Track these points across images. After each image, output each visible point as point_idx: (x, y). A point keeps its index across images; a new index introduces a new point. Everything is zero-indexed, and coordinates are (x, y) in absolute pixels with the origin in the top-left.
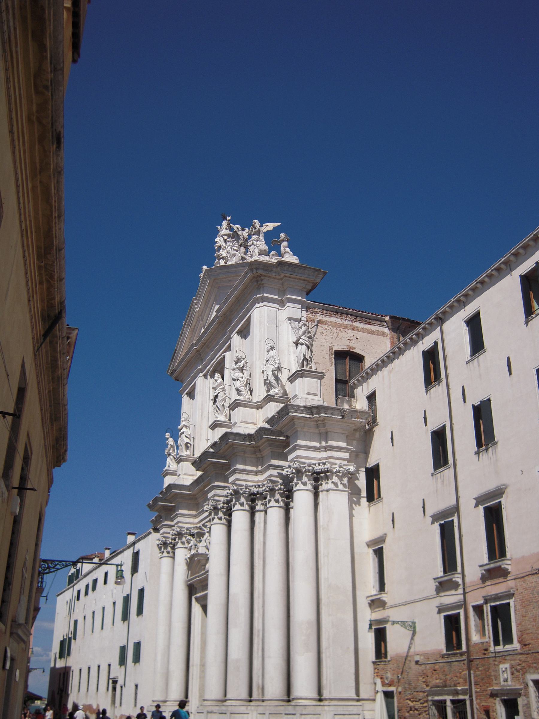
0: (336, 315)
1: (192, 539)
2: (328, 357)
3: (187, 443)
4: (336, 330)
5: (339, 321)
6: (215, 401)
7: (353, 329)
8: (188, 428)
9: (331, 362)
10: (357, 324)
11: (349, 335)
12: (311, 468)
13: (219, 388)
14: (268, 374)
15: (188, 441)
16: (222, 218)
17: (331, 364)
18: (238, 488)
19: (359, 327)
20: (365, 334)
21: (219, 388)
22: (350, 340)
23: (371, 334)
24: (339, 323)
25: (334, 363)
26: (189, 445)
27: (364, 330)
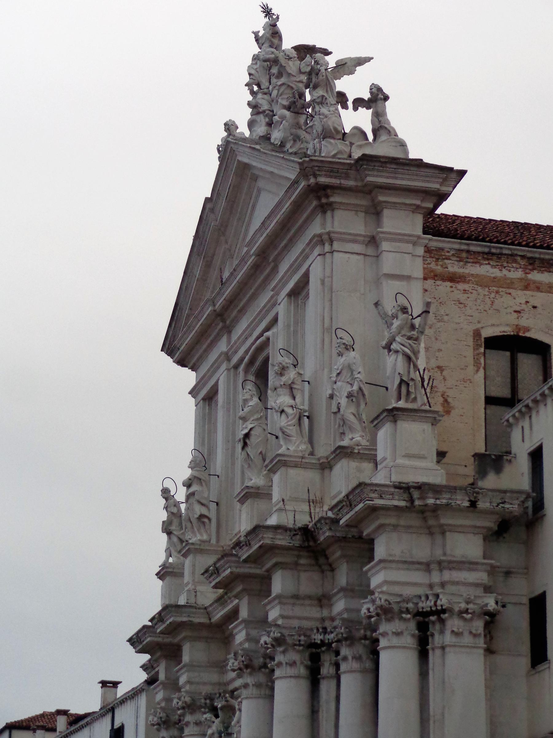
0: (488, 259)
1: (214, 719)
2: (469, 353)
3: (202, 516)
4: (487, 293)
5: (496, 272)
6: (245, 445)
8: (204, 484)
9: (477, 364)
10: (536, 276)
11: (518, 300)
12: (410, 605)
13: (252, 419)
14: (339, 403)
15: (204, 511)
16: (264, 12)
17: (476, 369)
18: (283, 635)
19: (541, 283)
21: (252, 419)
24: (494, 278)
25: (483, 365)
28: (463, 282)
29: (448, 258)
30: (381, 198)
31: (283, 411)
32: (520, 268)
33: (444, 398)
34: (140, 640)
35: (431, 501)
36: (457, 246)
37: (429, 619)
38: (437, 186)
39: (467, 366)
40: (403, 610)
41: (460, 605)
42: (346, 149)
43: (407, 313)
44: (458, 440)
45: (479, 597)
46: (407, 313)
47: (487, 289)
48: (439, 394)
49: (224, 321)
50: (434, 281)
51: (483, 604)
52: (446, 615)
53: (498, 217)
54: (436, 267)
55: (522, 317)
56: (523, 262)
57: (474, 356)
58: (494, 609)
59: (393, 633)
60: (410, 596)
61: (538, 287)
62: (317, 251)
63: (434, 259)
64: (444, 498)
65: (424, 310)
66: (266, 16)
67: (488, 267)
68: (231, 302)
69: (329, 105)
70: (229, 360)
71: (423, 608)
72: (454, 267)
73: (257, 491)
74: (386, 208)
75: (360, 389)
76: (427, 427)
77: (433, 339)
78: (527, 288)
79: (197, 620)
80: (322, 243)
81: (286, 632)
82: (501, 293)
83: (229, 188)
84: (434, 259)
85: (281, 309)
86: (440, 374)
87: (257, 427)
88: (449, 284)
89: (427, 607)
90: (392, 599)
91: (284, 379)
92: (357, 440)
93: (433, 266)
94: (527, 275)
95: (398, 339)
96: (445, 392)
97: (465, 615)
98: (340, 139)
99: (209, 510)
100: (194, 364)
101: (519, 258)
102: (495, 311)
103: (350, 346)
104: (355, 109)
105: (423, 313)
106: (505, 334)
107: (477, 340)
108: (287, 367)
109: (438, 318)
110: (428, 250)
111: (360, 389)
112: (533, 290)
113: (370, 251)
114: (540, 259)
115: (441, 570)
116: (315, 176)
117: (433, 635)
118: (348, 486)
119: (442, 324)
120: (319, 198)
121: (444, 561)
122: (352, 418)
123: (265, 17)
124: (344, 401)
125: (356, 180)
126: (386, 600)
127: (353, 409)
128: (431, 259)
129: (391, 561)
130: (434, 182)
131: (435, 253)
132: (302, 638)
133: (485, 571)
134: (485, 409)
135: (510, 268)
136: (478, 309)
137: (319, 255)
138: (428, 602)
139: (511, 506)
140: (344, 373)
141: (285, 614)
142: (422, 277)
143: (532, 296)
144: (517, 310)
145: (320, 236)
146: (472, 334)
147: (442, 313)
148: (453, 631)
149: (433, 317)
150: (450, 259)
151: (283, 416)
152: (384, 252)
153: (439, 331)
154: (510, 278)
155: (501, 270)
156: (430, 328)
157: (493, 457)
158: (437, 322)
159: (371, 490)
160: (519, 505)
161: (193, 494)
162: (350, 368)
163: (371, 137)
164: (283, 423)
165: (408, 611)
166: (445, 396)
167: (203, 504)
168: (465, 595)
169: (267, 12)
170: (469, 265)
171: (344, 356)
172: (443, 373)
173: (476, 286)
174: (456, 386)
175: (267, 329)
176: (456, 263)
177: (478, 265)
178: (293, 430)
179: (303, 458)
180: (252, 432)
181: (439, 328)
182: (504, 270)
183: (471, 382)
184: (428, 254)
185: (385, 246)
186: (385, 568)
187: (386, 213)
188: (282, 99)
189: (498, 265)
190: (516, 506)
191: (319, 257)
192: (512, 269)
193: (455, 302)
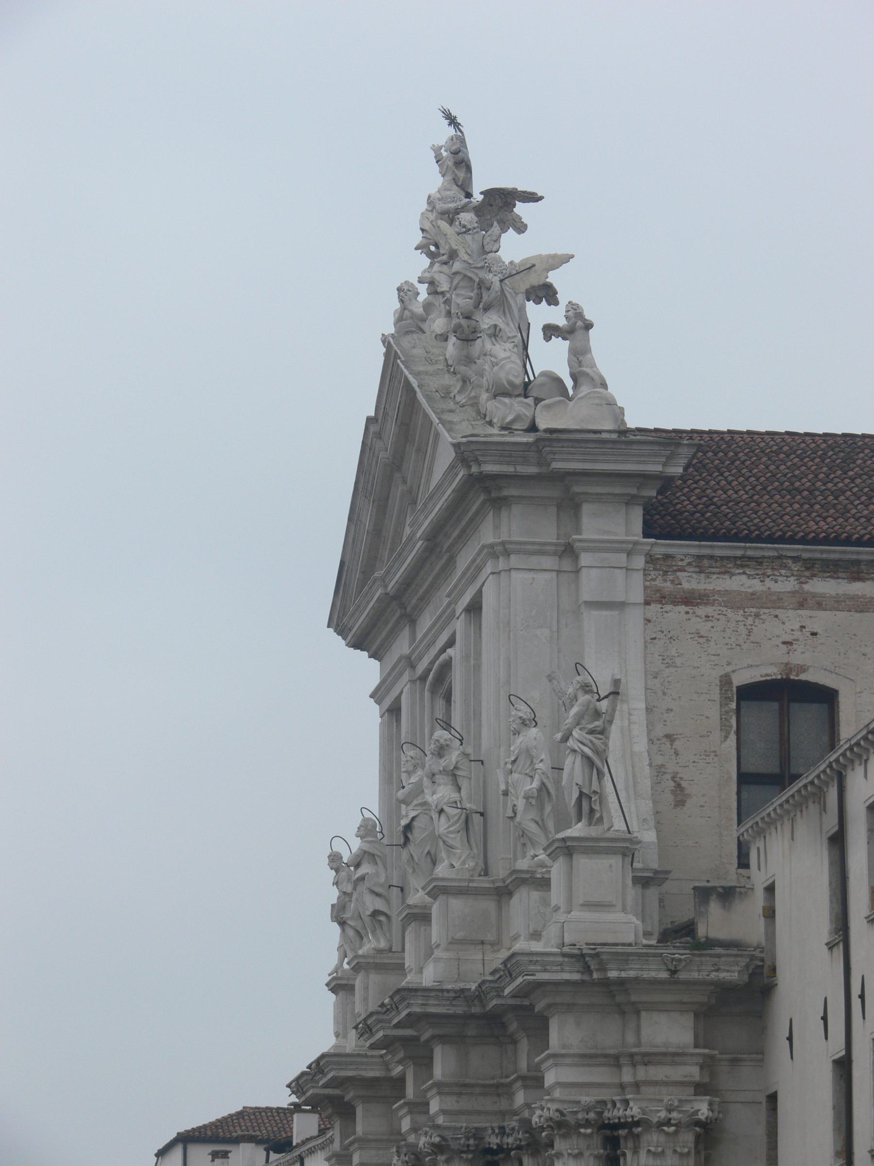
0: (742, 566)
2: (714, 712)
3: (376, 913)
4: (742, 618)
5: (755, 585)
7: (801, 605)
13: (415, 802)
14: (515, 805)
15: (380, 905)
17: (723, 734)
18: (443, 1138)
19: (823, 596)
20: (841, 616)
21: (415, 802)
22: (790, 643)
23: (860, 612)
24: (753, 594)
26: (382, 918)
27: (839, 603)
28: (705, 603)
29: (682, 570)
30: (577, 489)
31: (441, 811)
32: (793, 575)
33: (675, 782)
34: (302, 1090)
35: (613, 974)
36: (694, 551)
37: (618, 1134)
38: (659, 468)
39: (711, 732)
40: (581, 1123)
41: (658, 1115)
42: (528, 414)
43: (591, 691)
44: (697, 843)
45: (687, 1101)
46: (591, 691)
47: (741, 612)
48: (669, 776)
49: (403, 606)
50: (660, 606)
51: (692, 1110)
52: (640, 1129)
53: (819, 428)
54: (665, 585)
55: (795, 650)
56: (796, 567)
57: (721, 715)
58: (707, 1118)
59: (569, 1154)
60: (591, 1104)
61: (820, 604)
62: (489, 568)
63: (661, 573)
64: (631, 969)
65: (612, 689)
66: (450, 124)
67: (744, 578)
68: (408, 583)
69: (505, 338)
70: (413, 667)
71: (609, 1119)
72: (690, 582)
73: (423, 911)
74: (585, 501)
75: (543, 784)
76: (616, 861)
77: (660, 694)
78: (803, 606)
79: (371, 1074)
80: (495, 556)
81: (448, 1134)
82: (763, 617)
83: (399, 408)
84: (661, 573)
85: (459, 625)
86: (670, 747)
87: (421, 815)
88: (683, 608)
89: (614, 1118)
90: (567, 1108)
91: (443, 762)
92: (540, 860)
93: (659, 583)
94: (804, 586)
95: (576, 733)
96: (677, 773)
97: (665, 1128)
98: (519, 395)
99: (387, 901)
100: (379, 649)
101: (790, 561)
102: (753, 645)
103: (529, 720)
104: (547, 338)
105: (610, 694)
106: (769, 678)
107: (726, 691)
108: (447, 745)
109: (665, 662)
110: (651, 559)
111: (543, 784)
112: (812, 609)
113: (567, 565)
114: (822, 560)
115: (634, 1065)
116: (479, 464)
117: (624, 1155)
118: (529, 926)
119: (672, 670)
120: (487, 490)
121: (636, 1054)
122: (533, 828)
123: (449, 125)
124: (521, 804)
125: (539, 464)
126: (557, 1110)
127: (533, 814)
128: (656, 573)
129: (563, 1056)
130: (654, 463)
131: (662, 562)
132: (471, 1142)
133: (697, 1064)
134: (739, 793)
135: (777, 578)
136: (727, 644)
137: (493, 573)
138: (615, 1112)
139: (729, 974)
140: (521, 761)
141: (445, 1107)
142: (643, 602)
143: (811, 617)
144: (787, 640)
145: (492, 546)
146: (718, 683)
147: (673, 654)
148: (649, 1151)
149: (659, 660)
150: (685, 571)
151: (443, 818)
152: (583, 569)
153: (669, 682)
154: (776, 592)
155: (762, 581)
156: (655, 677)
157: (720, 890)
158: (666, 667)
159: (531, 961)
160: (739, 972)
161: (362, 878)
162: (528, 753)
163: (569, 383)
164: (443, 829)
165: (587, 1123)
166: (677, 779)
167: (378, 895)
168: (666, 1100)
169: (452, 121)
170: (715, 576)
171: (521, 735)
172: (675, 744)
173: (724, 609)
174: (694, 762)
175: (443, 650)
176: (694, 575)
177: (727, 576)
178: (456, 840)
179: (470, 881)
180: (415, 823)
181: (668, 677)
182: (767, 580)
183: (716, 756)
184: (651, 565)
185: (585, 559)
186: (556, 1065)
187: (587, 509)
188: (457, 295)
189: (757, 574)
190: (736, 974)
191: (491, 577)
192: (780, 578)
193: (692, 636)
